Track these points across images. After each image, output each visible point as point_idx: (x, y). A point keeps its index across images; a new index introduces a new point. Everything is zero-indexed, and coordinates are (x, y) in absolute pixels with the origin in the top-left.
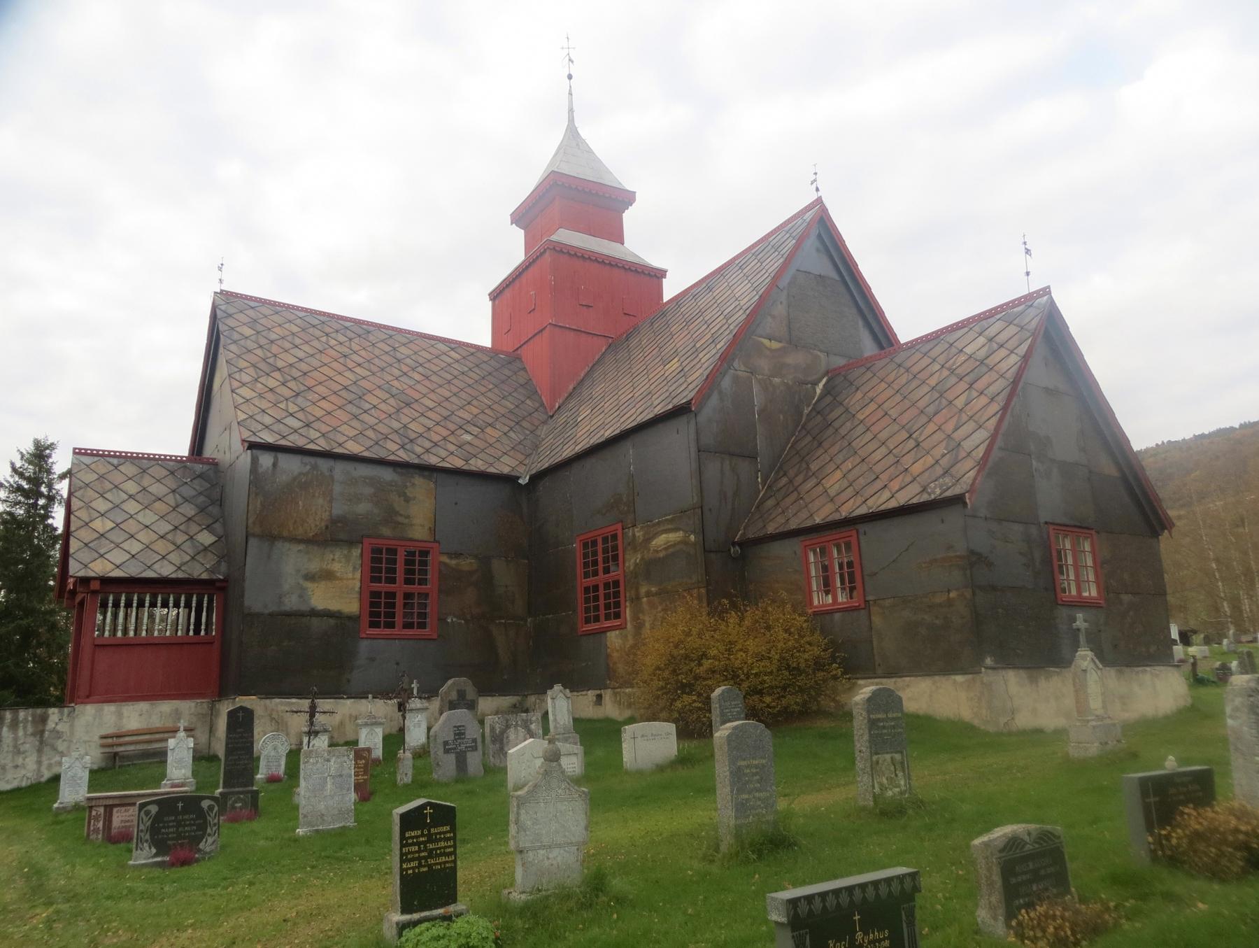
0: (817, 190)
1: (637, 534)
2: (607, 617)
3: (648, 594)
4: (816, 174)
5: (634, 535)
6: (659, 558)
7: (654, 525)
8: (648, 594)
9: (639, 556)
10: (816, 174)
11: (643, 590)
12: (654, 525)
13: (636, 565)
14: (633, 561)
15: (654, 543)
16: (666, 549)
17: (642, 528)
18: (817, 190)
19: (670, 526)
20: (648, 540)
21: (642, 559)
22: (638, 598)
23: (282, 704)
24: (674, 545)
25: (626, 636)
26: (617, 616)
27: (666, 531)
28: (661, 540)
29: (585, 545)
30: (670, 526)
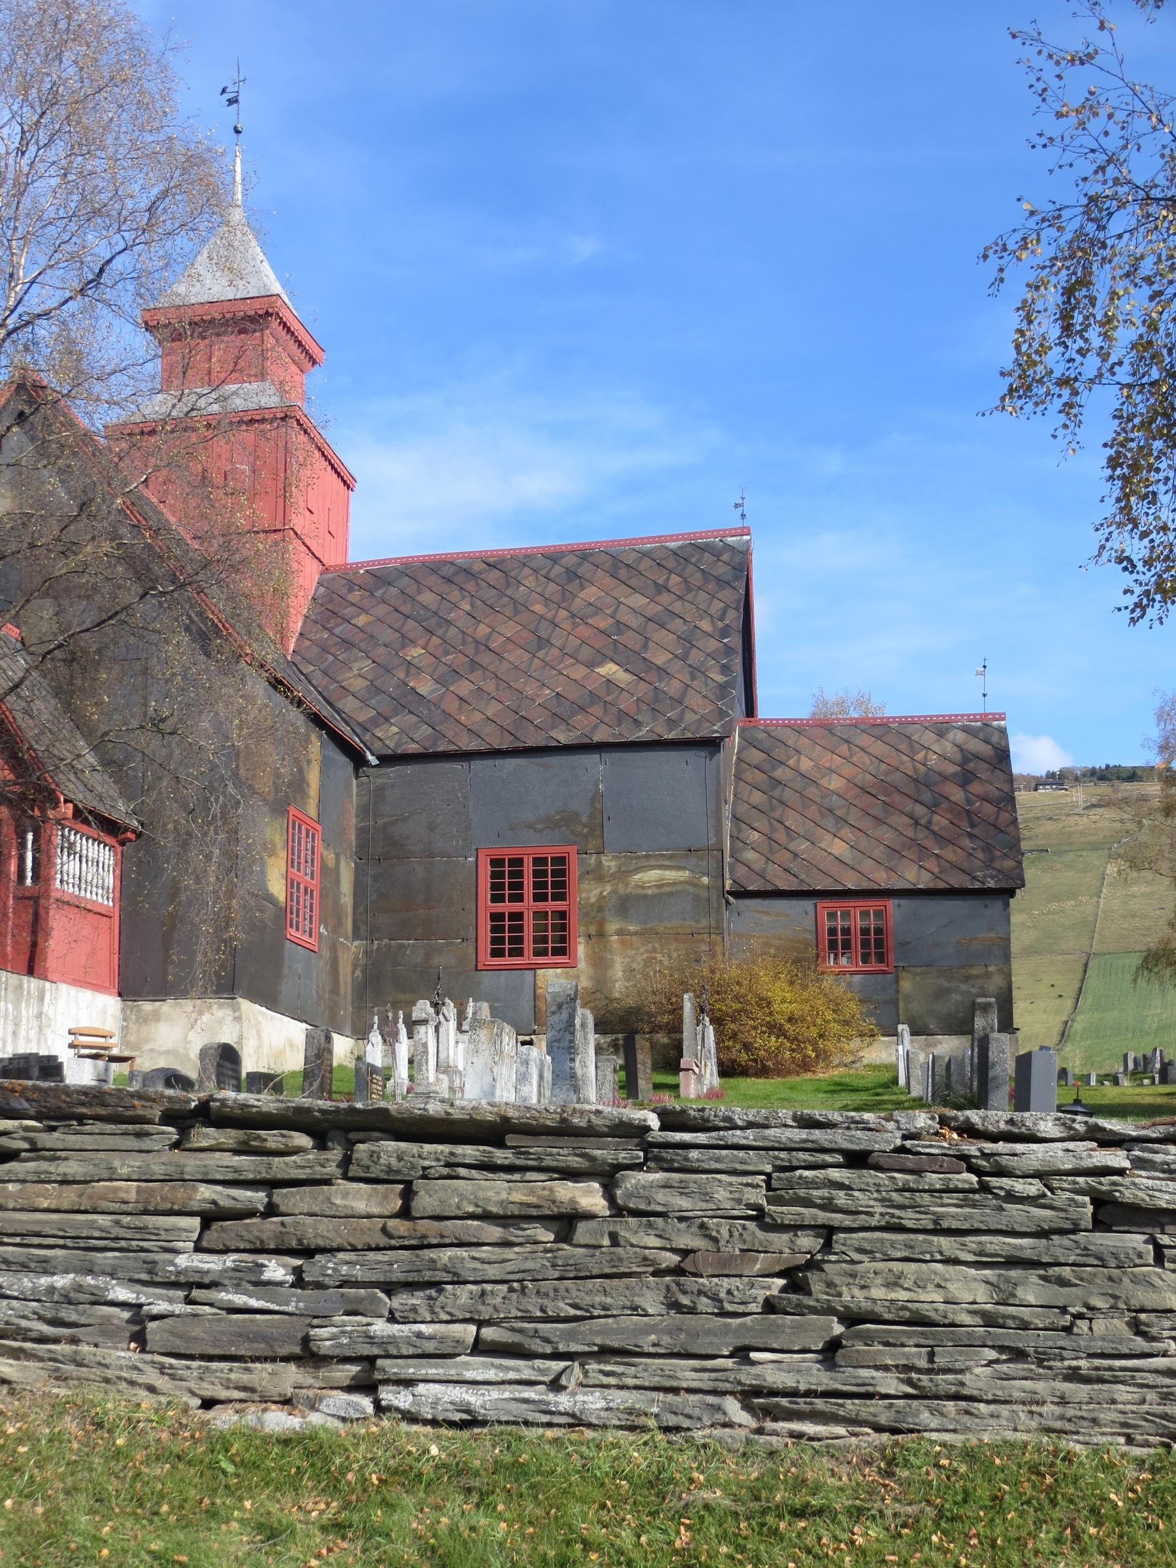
0: (743, 516)
1: (606, 864)
2: (538, 953)
3: (620, 933)
4: (743, 498)
5: (599, 864)
6: (645, 896)
7: (638, 858)
8: (620, 933)
9: (608, 888)
10: (743, 498)
11: (612, 926)
12: (638, 858)
13: (601, 897)
14: (595, 892)
15: (637, 877)
16: (657, 886)
17: (616, 858)
18: (743, 516)
19: (667, 863)
20: (622, 874)
21: (614, 892)
22: (601, 934)
23: (263, 1014)
24: (674, 884)
25: (578, 977)
26: (558, 952)
27: (660, 867)
28: (652, 876)
29: (496, 862)
30: (667, 863)
